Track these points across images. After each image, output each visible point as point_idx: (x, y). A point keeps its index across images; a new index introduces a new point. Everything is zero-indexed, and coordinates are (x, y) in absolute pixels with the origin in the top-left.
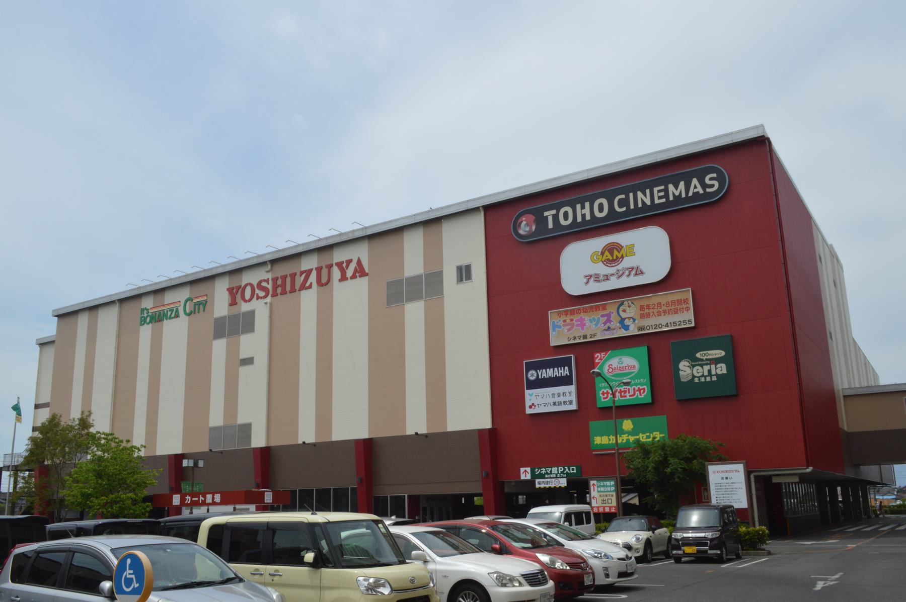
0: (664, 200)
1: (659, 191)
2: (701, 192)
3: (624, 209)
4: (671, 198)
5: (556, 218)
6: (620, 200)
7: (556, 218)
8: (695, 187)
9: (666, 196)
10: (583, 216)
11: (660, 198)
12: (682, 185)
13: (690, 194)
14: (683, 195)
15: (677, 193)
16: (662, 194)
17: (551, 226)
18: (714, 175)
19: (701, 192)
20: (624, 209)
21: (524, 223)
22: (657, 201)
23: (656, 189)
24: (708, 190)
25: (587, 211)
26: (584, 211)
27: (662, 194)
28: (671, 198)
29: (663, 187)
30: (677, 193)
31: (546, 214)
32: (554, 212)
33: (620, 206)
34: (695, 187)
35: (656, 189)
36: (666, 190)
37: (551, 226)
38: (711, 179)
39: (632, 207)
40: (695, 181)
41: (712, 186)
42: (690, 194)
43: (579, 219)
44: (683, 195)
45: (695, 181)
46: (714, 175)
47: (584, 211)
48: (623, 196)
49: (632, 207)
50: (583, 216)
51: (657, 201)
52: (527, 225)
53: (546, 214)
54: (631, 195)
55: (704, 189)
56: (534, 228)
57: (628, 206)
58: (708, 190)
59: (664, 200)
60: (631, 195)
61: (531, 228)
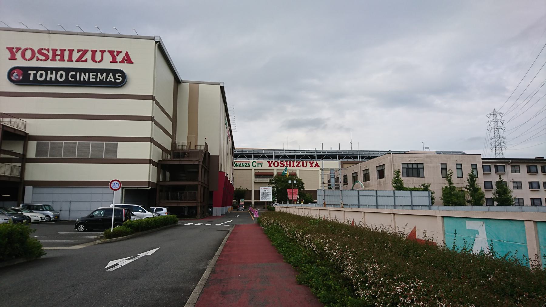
0: (94, 80)
1: (93, 75)
2: (113, 81)
3: (74, 80)
4: (98, 80)
5: (35, 75)
6: (72, 75)
7: (35, 75)
8: (111, 78)
9: (96, 78)
10: (51, 78)
11: (93, 78)
12: (105, 75)
13: (108, 80)
14: (104, 80)
15: (101, 79)
16: (94, 77)
17: (31, 79)
18: (121, 75)
19: (113, 81)
20: (74, 80)
21: (15, 74)
22: (91, 80)
23: (91, 74)
24: (116, 81)
25: (53, 76)
26: (51, 76)
27: (94, 77)
28: (98, 80)
29: (95, 74)
30: (101, 79)
31: (30, 72)
32: (35, 72)
33: (72, 78)
34: (111, 78)
35: (91, 74)
36: (96, 76)
37: (31, 79)
38: (119, 76)
39: (78, 79)
40: (111, 75)
41: (119, 79)
42: (108, 80)
43: (48, 79)
44: (104, 80)
45: (111, 75)
46: (121, 75)
47: (51, 76)
48: (74, 73)
49: (78, 79)
50: (51, 78)
51: (91, 80)
52: (17, 75)
53: (30, 72)
54: (78, 73)
55: (115, 80)
56: (21, 78)
57: (76, 79)
58: (116, 81)
59: (94, 80)
60: (78, 73)
61: (19, 77)
